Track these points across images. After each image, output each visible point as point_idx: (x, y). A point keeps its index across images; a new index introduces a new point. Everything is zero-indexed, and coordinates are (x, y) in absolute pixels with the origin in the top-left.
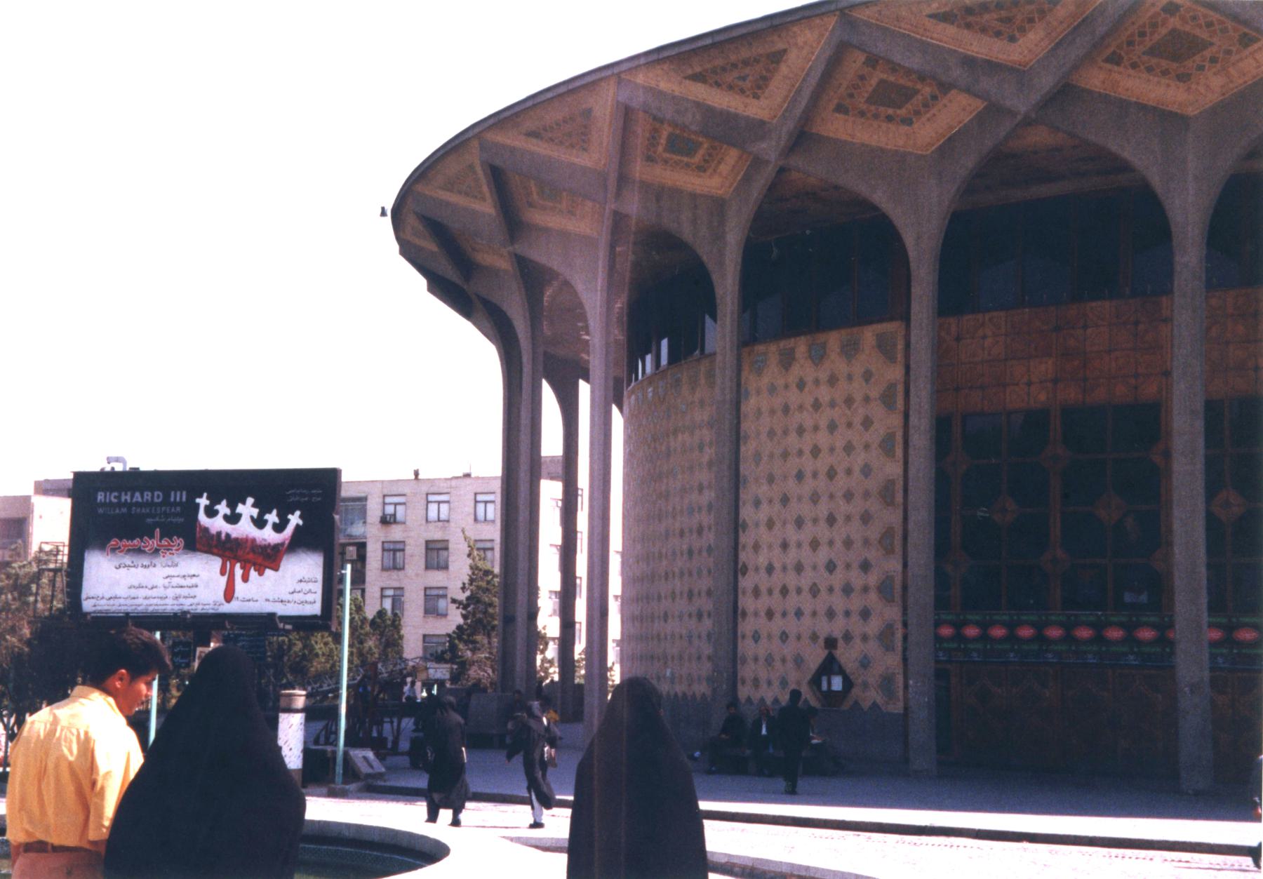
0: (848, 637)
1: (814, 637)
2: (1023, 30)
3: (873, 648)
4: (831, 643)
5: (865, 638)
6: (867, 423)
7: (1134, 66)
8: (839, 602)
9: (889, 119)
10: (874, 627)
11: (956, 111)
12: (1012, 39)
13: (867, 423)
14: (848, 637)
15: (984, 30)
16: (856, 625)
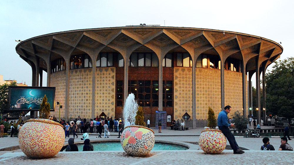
0: (106, 110)
1: (100, 110)
2: (144, 34)
3: (110, 111)
4: (103, 110)
5: (109, 110)
6: (109, 80)
7: (156, 41)
8: (105, 105)
9: (123, 42)
10: (110, 108)
11: (131, 43)
12: (143, 35)
13: (109, 80)
14: (106, 110)
15: (140, 34)
16: (107, 108)
